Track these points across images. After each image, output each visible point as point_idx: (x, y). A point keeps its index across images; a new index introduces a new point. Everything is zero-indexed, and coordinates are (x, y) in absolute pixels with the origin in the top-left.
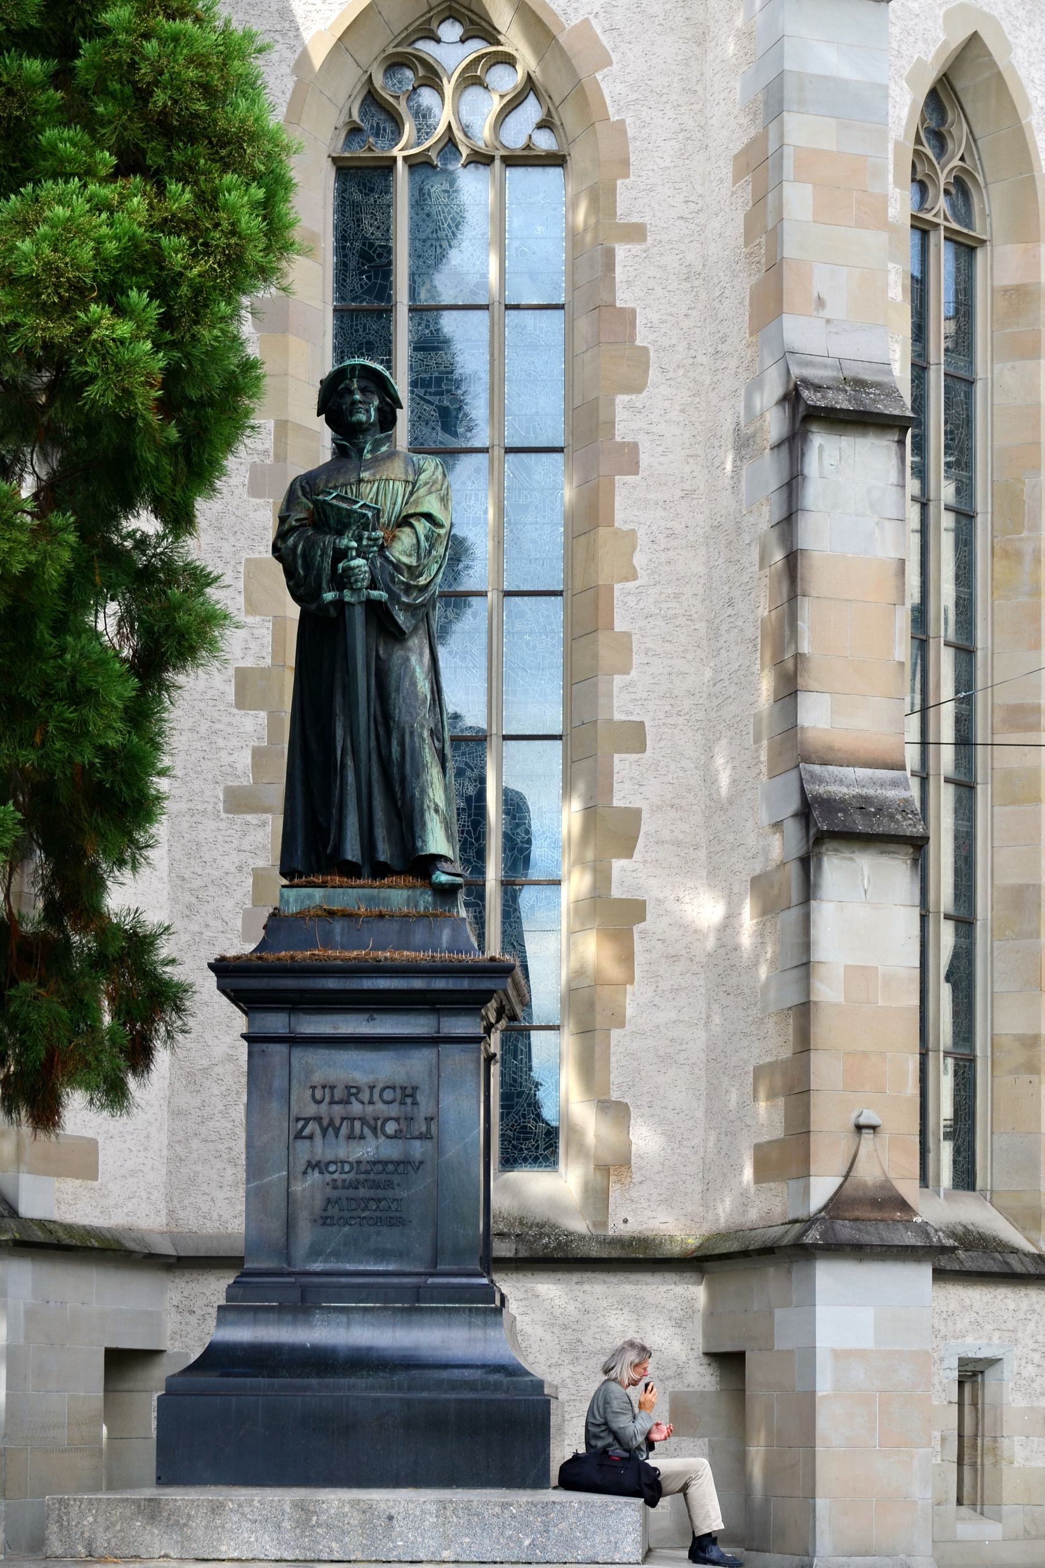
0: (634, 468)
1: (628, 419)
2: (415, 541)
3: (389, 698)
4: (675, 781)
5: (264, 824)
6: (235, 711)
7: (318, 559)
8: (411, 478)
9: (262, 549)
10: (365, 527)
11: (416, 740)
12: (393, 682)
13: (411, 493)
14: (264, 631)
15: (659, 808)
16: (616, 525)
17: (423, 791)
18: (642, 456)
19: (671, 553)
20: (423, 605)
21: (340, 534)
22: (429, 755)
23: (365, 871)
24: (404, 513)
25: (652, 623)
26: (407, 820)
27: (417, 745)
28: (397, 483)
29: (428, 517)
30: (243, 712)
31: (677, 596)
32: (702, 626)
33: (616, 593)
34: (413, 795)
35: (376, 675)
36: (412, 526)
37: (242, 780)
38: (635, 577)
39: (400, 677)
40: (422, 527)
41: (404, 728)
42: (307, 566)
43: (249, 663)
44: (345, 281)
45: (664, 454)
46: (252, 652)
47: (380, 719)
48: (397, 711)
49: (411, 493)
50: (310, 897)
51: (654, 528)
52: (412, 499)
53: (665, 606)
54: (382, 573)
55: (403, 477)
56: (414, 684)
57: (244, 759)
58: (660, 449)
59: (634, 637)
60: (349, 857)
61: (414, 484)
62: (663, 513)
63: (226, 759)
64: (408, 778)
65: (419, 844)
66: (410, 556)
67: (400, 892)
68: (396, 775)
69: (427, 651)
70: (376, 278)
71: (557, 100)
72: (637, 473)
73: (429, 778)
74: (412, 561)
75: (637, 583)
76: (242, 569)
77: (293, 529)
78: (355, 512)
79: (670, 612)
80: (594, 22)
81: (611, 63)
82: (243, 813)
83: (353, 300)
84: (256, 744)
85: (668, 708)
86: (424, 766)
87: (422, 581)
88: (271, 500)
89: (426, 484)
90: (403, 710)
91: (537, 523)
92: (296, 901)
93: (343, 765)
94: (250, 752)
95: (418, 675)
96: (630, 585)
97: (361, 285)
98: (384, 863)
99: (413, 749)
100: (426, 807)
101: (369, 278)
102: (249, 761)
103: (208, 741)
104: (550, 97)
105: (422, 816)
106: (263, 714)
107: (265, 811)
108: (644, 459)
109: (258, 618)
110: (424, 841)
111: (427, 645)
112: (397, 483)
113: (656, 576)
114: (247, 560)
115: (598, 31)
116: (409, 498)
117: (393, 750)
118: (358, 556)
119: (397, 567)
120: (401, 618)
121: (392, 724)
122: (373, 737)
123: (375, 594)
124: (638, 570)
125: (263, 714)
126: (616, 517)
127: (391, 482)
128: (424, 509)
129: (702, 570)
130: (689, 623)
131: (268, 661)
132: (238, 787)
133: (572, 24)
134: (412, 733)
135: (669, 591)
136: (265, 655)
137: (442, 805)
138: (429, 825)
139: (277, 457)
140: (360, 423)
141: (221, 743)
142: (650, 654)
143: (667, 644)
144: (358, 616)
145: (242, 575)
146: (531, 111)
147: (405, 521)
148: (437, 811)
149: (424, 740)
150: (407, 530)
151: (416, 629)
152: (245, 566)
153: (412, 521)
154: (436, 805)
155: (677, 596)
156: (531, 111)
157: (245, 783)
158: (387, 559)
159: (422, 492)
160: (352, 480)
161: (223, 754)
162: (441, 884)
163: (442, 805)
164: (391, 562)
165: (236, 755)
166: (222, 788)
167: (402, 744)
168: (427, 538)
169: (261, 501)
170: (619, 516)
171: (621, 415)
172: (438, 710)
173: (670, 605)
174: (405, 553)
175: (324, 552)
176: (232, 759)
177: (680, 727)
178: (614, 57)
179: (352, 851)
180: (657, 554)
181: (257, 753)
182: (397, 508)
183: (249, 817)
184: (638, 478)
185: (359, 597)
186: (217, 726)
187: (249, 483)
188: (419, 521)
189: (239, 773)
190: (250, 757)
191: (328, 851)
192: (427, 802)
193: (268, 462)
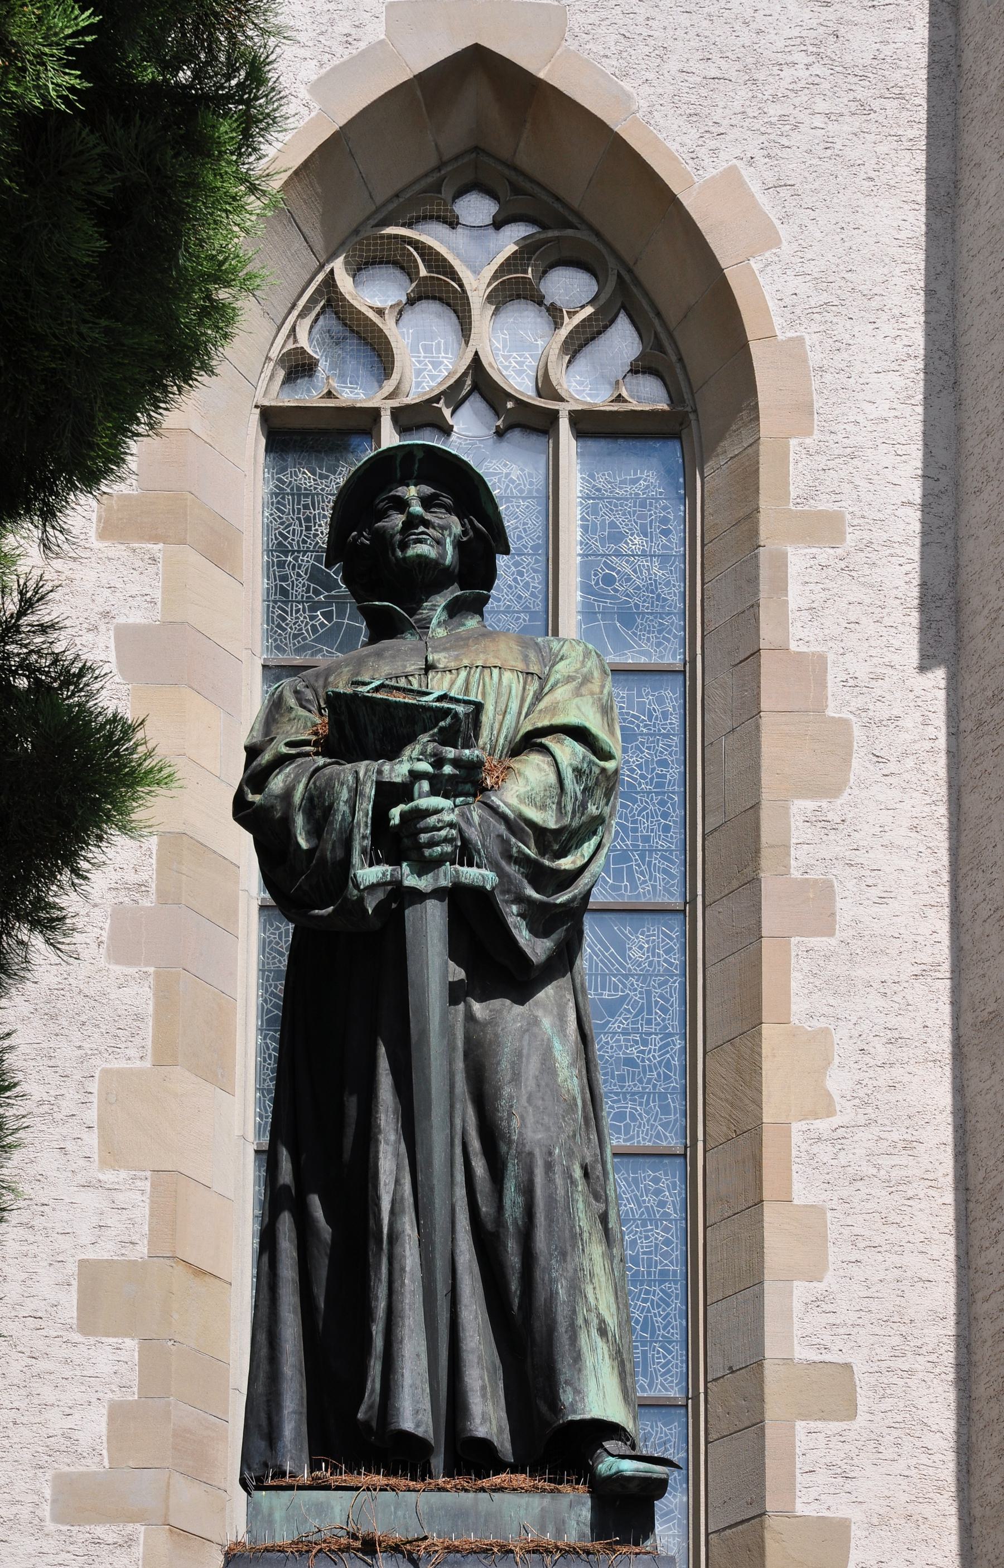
2: (552, 778)
3: (497, 1096)
4: (913, 1472)
5: (129, 1542)
6: (77, 1337)
7: (343, 808)
8: (534, 668)
9: (132, 1052)
11: (559, 1181)
12: (505, 1065)
13: (538, 697)
14: (137, 1196)
15: (884, 1521)
16: (794, 1020)
17: (576, 1289)
18: (839, 904)
19: (897, 1072)
21: (393, 754)
23: (438, 1462)
24: (527, 727)
25: (864, 1190)
27: (561, 1192)
28: (507, 676)
29: (580, 734)
30: (92, 1340)
33: (796, 1138)
34: (552, 1296)
35: (466, 1055)
36: (545, 750)
37: (88, 1461)
38: (830, 1112)
39: (520, 1055)
40: (568, 752)
41: (531, 1154)
42: (318, 827)
43: (104, 1251)
44: (284, 619)
45: (882, 901)
46: (111, 1233)
47: (475, 1144)
48: (516, 1123)
49: (538, 697)
50: (321, 1509)
51: (865, 1026)
52: (542, 705)
53: (886, 1161)
54: (484, 835)
55: (521, 666)
57: (94, 1426)
58: (874, 893)
59: (829, 1214)
60: (408, 1425)
61: (543, 680)
62: (881, 1002)
63: (57, 1423)
64: (542, 1261)
65: (567, 1397)
66: (543, 807)
67: (523, 1500)
68: (513, 1257)
69: (572, 1016)
70: (341, 614)
71: (672, 316)
72: (831, 933)
73: (586, 1263)
75: (836, 1121)
76: (94, 1087)
77: (280, 761)
78: (430, 709)
79: (895, 1174)
80: (747, 173)
81: (777, 242)
82: (90, 1522)
83: (299, 651)
84: (117, 1396)
85: (896, 1340)
86: (575, 1237)
87: (566, 863)
88: (151, 970)
89: (569, 679)
90: (530, 1120)
91: (636, 1030)
92: (288, 1519)
93: (394, 1237)
94: (105, 1411)
95: (557, 1054)
96: (823, 1125)
97: (313, 626)
98: (485, 1444)
99: (551, 1200)
100: (580, 1321)
101: (328, 616)
102: (102, 1428)
103: (23, 1392)
104: (658, 314)
105: (574, 1339)
106: (131, 1344)
107: (132, 1519)
108: (845, 910)
109: (123, 1174)
110: (577, 1392)
111: (572, 1004)
112: (507, 676)
113: (869, 1110)
114: (105, 1072)
115: (755, 188)
116: (533, 704)
117: (507, 1202)
118: (434, 792)
121: (504, 1148)
122: (460, 1177)
123: (471, 874)
124: (837, 1098)
125: (131, 1344)
126: (794, 1008)
127: (496, 672)
128: (572, 718)
130: (931, 1192)
131: (142, 1250)
132: (82, 1474)
133: (708, 176)
134: (549, 1167)
135: (895, 1136)
136: (135, 1238)
137: (612, 1323)
138: (589, 1360)
139: (163, 897)
141: (49, 1395)
142: (861, 1245)
143: (892, 1229)
144: (430, 928)
145: (94, 1099)
147: (530, 742)
148: (603, 1332)
149: (573, 1182)
150: (536, 759)
152: (101, 1083)
153: (545, 741)
154: (602, 1322)
157: (94, 1468)
158: (493, 810)
159: (561, 693)
160: (410, 668)
161: (53, 1415)
162: (619, 1479)
164: (503, 817)
165: (77, 1416)
166: (49, 1476)
167: (528, 1191)
168: (578, 772)
169: (132, 970)
170: (798, 1006)
171: (799, 832)
172: (594, 1137)
173: (895, 1160)
174: (531, 800)
175: (356, 792)
176: (69, 1422)
177: (920, 1375)
178: (783, 231)
179: (415, 1412)
180: (871, 1073)
181: (117, 1413)
182: (510, 720)
183: (99, 1530)
184: (833, 941)
185: (436, 879)
186: (42, 1365)
187: (110, 938)
188: (560, 742)
189: (83, 1448)
190: (105, 1419)
191: (360, 1416)
192: (582, 1312)
193: (146, 903)
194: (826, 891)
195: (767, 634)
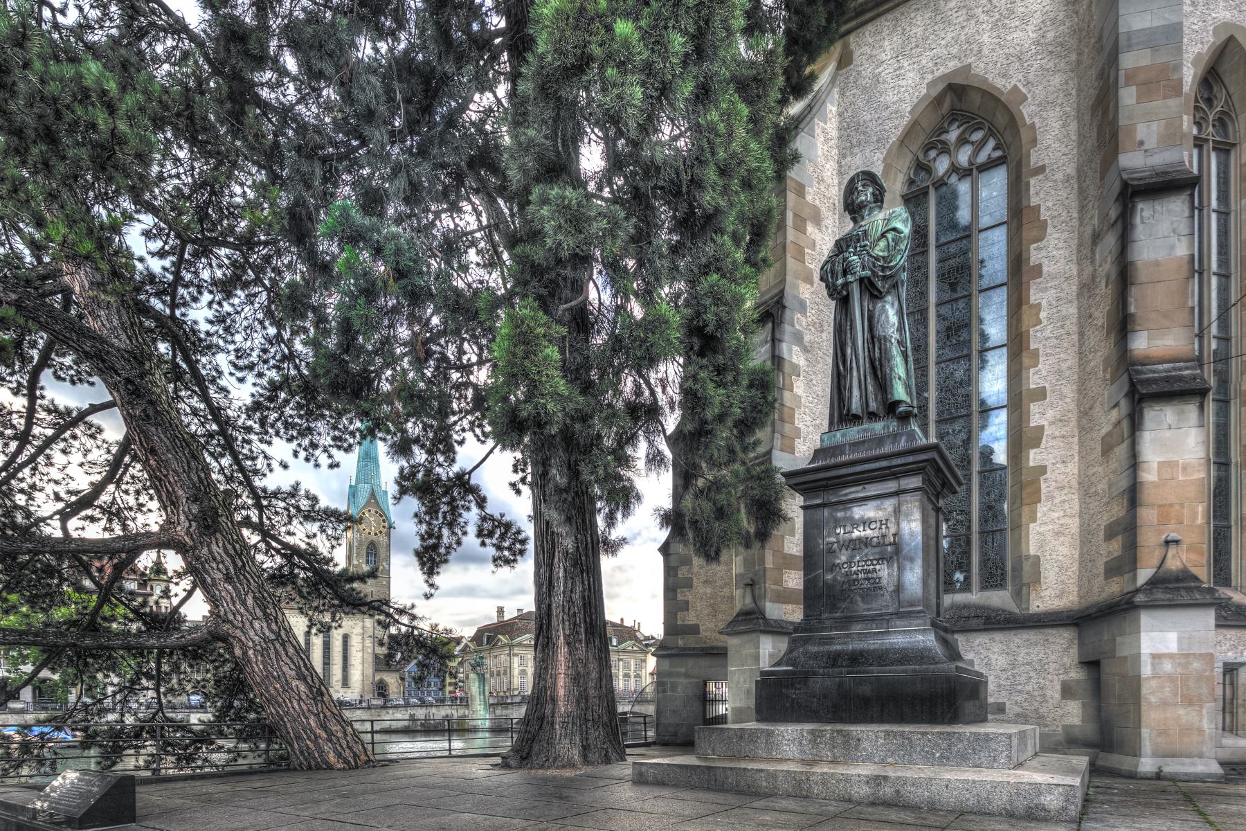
0: (1040, 274)
1: (1035, 255)
10: (858, 241)
20: (891, 276)
22: (895, 351)
26: (883, 385)
31: (1062, 326)
32: (1075, 337)
56: (887, 317)
74: (886, 254)
119: (877, 259)
120: (879, 284)
129: (1075, 311)
140: (862, 202)
146: (991, 143)
151: (888, 292)
155: (1062, 326)
156: (991, 143)
163: (903, 376)
194: (1040, 266)
195: (1025, 203)
